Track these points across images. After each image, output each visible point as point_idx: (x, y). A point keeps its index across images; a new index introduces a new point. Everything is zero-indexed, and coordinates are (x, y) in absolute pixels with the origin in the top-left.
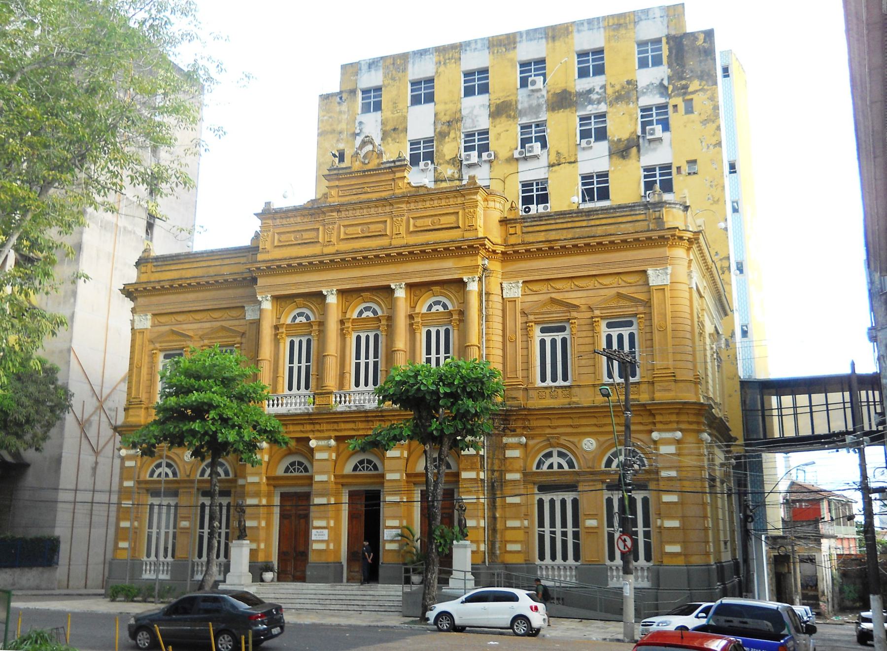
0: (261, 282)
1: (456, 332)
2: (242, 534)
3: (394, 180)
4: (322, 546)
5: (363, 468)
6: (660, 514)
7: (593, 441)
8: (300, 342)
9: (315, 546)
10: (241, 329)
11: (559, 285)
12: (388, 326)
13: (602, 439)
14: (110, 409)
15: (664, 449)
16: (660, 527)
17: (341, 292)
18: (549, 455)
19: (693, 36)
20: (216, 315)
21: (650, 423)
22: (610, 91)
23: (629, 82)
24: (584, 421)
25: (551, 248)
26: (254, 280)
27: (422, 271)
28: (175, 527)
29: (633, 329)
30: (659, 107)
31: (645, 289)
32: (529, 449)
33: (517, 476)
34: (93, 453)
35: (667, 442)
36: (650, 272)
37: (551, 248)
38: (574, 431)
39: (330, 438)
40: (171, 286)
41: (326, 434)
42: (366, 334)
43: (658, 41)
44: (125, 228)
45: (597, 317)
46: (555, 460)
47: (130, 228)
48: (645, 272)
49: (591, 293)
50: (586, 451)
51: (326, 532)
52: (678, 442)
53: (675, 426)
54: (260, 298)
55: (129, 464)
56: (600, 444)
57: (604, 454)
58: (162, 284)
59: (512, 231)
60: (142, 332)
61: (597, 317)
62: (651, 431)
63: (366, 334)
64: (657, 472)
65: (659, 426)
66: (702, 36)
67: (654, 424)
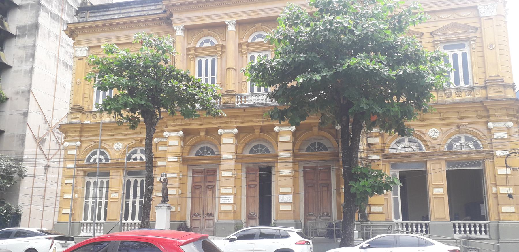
0: (175, 16)
4: (229, 208)
5: (258, 151)
6: (495, 184)
8: (207, 61)
9: (223, 208)
13: (444, 129)
15: (496, 135)
16: (496, 194)
17: (240, 24)
21: (484, 116)
26: (171, 15)
28: (107, 198)
29: (467, 50)
33: (378, 157)
35: (500, 130)
38: (422, 123)
39: (232, 128)
40: (104, 25)
41: (230, 125)
48: (476, 7)
49: (432, 25)
50: (434, 139)
52: (509, 129)
53: (506, 118)
54: (175, 28)
55: (70, 152)
56: (443, 133)
57: (447, 139)
58: (97, 23)
60: (81, 59)
61: (437, 41)
62: (487, 122)
64: (492, 153)
65: (491, 118)
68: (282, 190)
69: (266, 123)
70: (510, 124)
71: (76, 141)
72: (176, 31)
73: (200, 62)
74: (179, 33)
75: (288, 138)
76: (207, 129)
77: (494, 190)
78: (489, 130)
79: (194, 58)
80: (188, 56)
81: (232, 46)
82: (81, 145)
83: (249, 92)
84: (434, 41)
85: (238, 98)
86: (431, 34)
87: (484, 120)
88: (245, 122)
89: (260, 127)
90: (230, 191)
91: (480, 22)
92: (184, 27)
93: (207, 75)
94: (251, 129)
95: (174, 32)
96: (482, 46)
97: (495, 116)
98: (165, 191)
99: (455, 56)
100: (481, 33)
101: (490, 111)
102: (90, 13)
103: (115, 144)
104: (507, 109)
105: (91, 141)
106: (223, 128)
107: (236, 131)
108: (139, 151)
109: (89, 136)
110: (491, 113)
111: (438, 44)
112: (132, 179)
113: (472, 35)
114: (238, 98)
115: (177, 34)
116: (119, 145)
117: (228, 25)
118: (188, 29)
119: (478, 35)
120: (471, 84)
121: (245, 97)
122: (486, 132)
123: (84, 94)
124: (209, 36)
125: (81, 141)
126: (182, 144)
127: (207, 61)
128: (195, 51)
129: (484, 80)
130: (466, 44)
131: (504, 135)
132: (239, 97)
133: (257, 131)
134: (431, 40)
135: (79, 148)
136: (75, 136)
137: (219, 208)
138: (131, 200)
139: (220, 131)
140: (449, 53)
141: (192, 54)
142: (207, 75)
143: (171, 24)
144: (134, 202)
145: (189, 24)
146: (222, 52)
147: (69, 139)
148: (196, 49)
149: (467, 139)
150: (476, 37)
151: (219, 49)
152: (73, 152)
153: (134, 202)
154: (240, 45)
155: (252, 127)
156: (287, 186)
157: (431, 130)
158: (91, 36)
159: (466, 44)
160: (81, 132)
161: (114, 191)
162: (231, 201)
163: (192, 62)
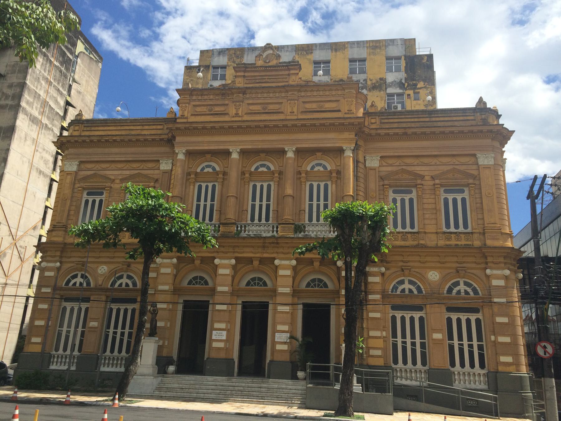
0: (178, 139)
1: (334, 186)
2: (153, 333)
3: (289, 75)
4: (221, 345)
6: (494, 332)
7: (436, 273)
9: (215, 345)
10: (156, 177)
11: (408, 161)
12: (279, 178)
14: (21, 247)
15: (495, 282)
16: (494, 342)
18: (402, 282)
19: (421, 57)
20: (135, 165)
21: (482, 263)
22: (369, 83)
23: (381, 79)
24: (428, 259)
25: (405, 134)
26: (174, 137)
27: (310, 140)
28: (84, 327)
30: (399, 95)
31: (475, 167)
32: (386, 277)
33: (378, 297)
34: (4, 276)
35: (498, 277)
36: (478, 155)
37: (405, 134)
38: (422, 265)
39: (231, 258)
41: (228, 255)
42: (261, 183)
43: (399, 58)
44: (46, 125)
45: (437, 184)
46: (407, 286)
47: (50, 126)
48: (474, 155)
49: (432, 168)
51: (224, 333)
52: (506, 278)
54: (177, 151)
55: (47, 274)
58: (92, 138)
59: (373, 121)
60: (69, 174)
61: (437, 184)
63: (261, 183)
66: (426, 58)
67: (487, 263)
68: (280, 327)
69: (265, 255)
70: (507, 272)
71: (55, 262)
72: (177, 154)
73: (200, 187)
74: (181, 157)
75: (288, 272)
76: (202, 257)
77: (493, 338)
78: (488, 277)
79: (194, 183)
80: (187, 180)
81: (234, 175)
82: (60, 267)
83: (249, 222)
84: (434, 185)
85: (237, 227)
86: (432, 177)
87: (483, 266)
88: (243, 253)
89: (259, 259)
90: (223, 326)
91: (479, 169)
92: (187, 151)
93: (206, 200)
94: (250, 261)
95: (175, 154)
96: (481, 193)
97: (493, 262)
98: (154, 323)
99: (455, 201)
100: (479, 180)
101: (488, 258)
102: (85, 126)
103: (100, 268)
104: (505, 257)
105: (73, 262)
106: (221, 258)
107: (233, 261)
108: (125, 277)
109: (71, 257)
110: (490, 259)
111: (437, 188)
112: (115, 307)
113: (471, 181)
114: (237, 227)
115: (178, 158)
116: (103, 269)
117: (231, 153)
118: (189, 154)
119: (477, 182)
120: (469, 230)
121: (245, 226)
122: (484, 279)
123: (69, 211)
124: (211, 161)
125: (61, 263)
126: (175, 273)
127: (207, 187)
128: (195, 175)
129: (482, 226)
130: (466, 189)
131: (502, 283)
132: (239, 226)
133: (256, 263)
134: (432, 183)
135: (59, 269)
136: (55, 256)
137: (210, 344)
138: (111, 330)
139: (217, 261)
140: (448, 197)
141: (193, 178)
142: (206, 200)
143: (173, 146)
144: (115, 333)
145: (191, 148)
146: (223, 179)
147: (48, 258)
148: (196, 174)
149: (466, 284)
150: (475, 184)
151: (221, 176)
152: (52, 274)
153: (115, 333)
154: (243, 173)
155: (251, 258)
156: (283, 324)
157: (431, 273)
158: (83, 151)
159: (466, 189)
160: (62, 252)
161: (94, 320)
162: (224, 338)
163: (192, 187)
